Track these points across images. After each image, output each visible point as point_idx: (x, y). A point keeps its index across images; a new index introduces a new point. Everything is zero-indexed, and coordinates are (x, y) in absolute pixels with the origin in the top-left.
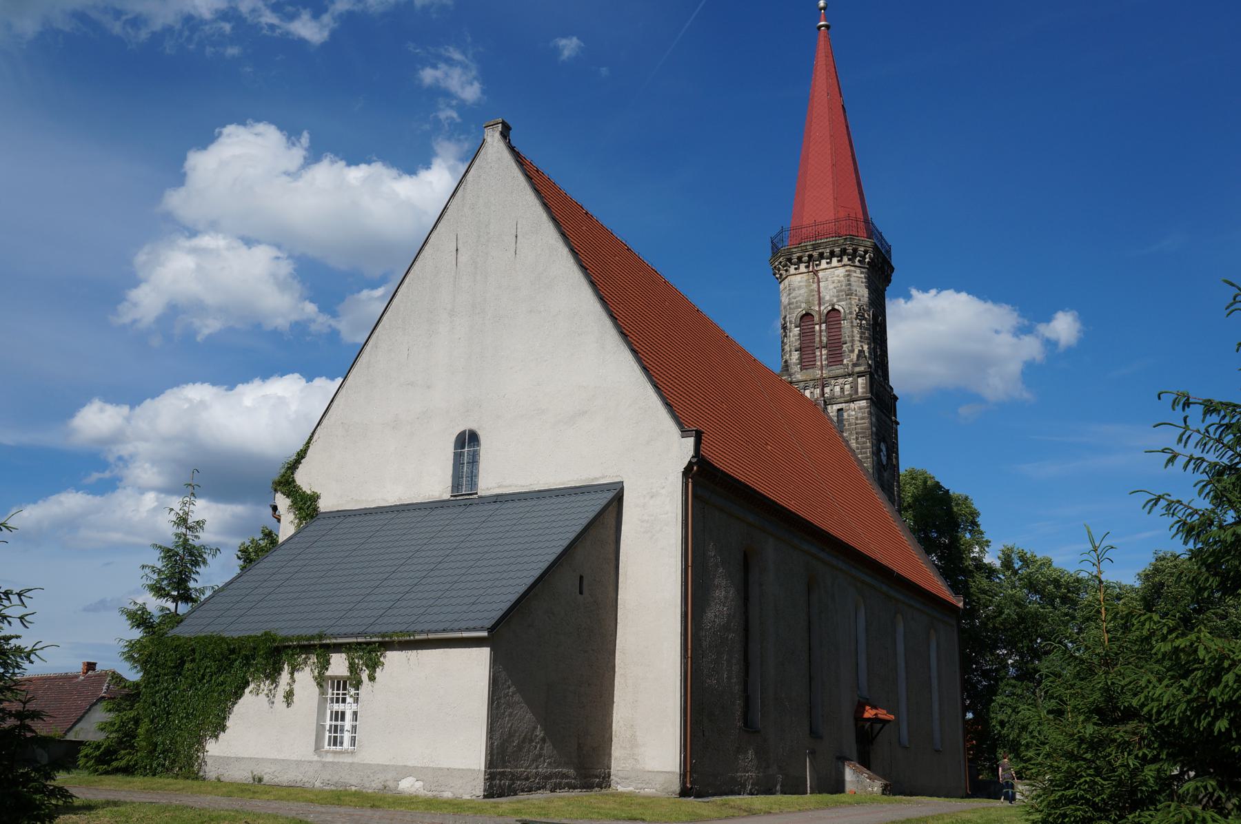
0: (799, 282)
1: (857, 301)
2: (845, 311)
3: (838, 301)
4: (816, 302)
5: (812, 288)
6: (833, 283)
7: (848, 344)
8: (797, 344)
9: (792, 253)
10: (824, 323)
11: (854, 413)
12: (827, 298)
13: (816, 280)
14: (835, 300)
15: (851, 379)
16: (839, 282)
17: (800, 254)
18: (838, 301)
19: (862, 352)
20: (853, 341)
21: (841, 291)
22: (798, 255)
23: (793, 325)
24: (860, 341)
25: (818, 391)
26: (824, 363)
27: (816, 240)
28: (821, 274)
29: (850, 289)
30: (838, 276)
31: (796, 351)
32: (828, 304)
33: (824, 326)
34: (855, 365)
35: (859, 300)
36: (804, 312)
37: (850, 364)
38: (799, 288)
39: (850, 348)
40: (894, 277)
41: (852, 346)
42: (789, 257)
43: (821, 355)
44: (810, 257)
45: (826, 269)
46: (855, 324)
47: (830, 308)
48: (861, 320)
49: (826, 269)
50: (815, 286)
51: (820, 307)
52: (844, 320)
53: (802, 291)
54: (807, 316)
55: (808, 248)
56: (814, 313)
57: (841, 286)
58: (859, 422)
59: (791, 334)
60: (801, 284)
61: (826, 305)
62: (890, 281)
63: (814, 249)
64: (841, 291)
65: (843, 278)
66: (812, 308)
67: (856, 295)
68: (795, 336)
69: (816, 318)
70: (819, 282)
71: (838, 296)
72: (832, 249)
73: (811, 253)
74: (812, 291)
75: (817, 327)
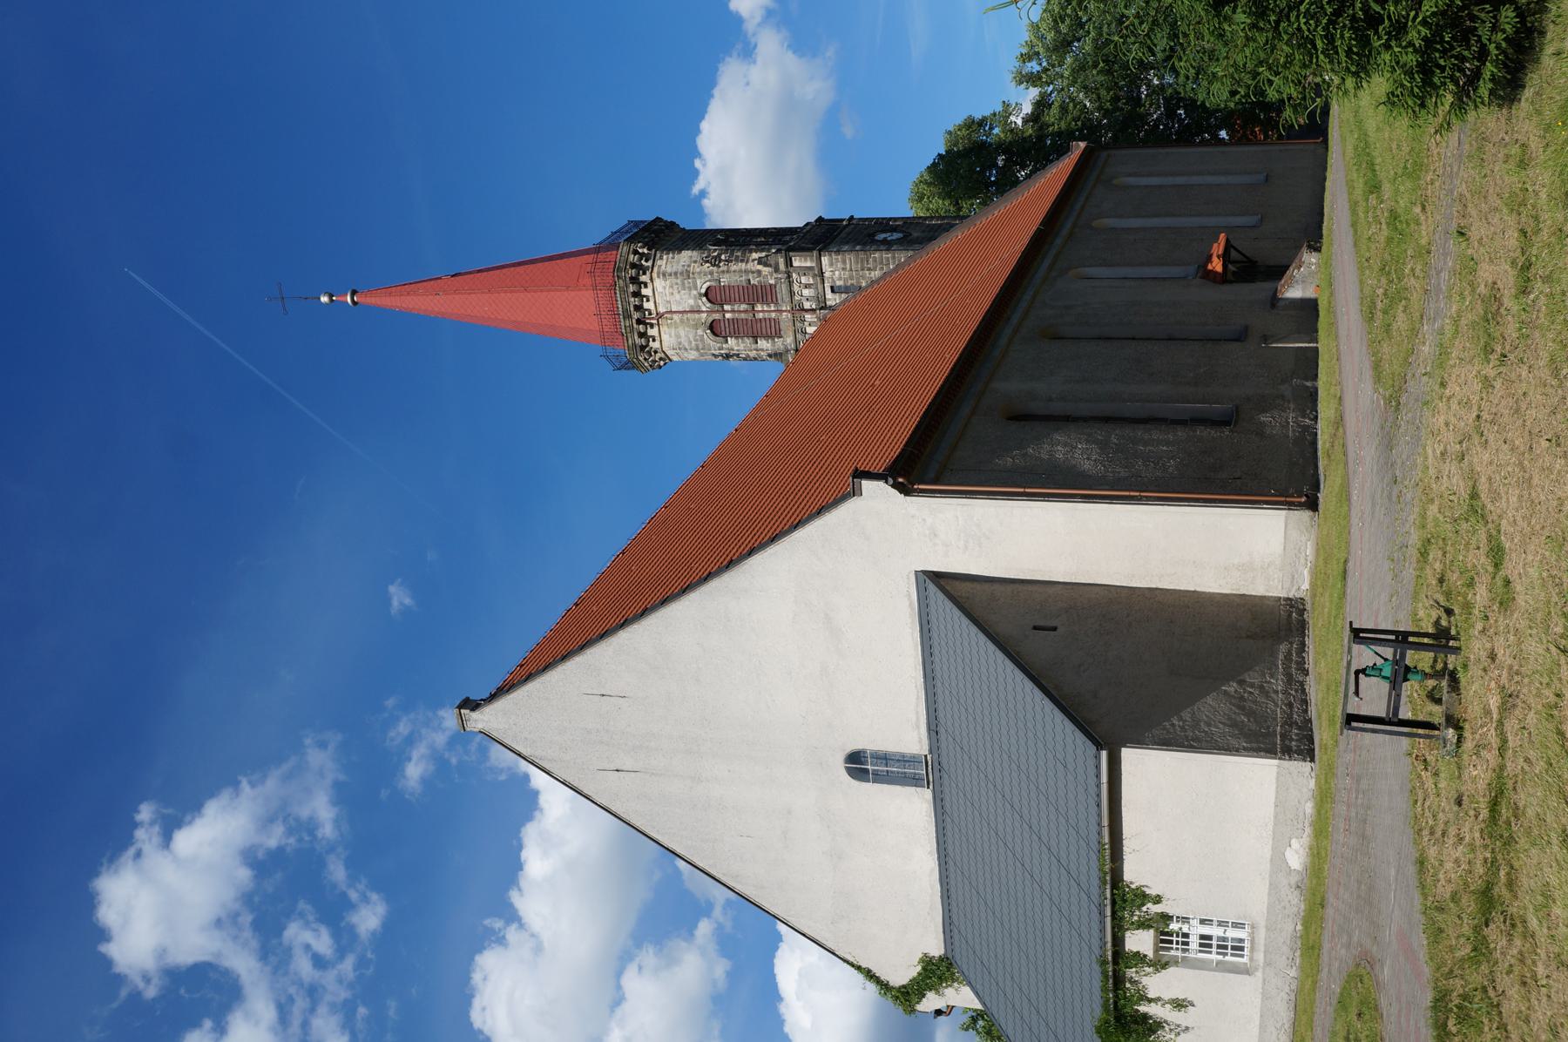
0: (670, 336)
1: (696, 265)
2: (709, 281)
3: (696, 288)
4: (697, 316)
5: (678, 321)
6: (672, 294)
7: (751, 277)
8: (748, 341)
9: (634, 344)
10: (723, 307)
11: (837, 273)
12: (691, 302)
13: (669, 316)
14: (695, 292)
15: (794, 275)
16: (671, 287)
17: (636, 334)
18: (696, 288)
19: (760, 261)
20: (746, 272)
21: (683, 284)
22: (636, 337)
23: (724, 346)
24: (747, 262)
25: (808, 317)
26: (773, 309)
27: (619, 314)
28: (662, 309)
29: (682, 273)
30: (665, 288)
31: (757, 343)
32: (700, 301)
33: (726, 307)
34: (777, 270)
35: (695, 262)
36: (709, 331)
38: (678, 336)
40: (668, 217)
41: (753, 272)
42: (638, 349)
43: (763, 311)
44: (639, 322)
45: (655, 302)
46: (725, 268)
47: (704, 299)
48: (720, 261)
49: (655, 302)
50: (676, 317)
51: (703, 312)
52: (720, 281)
53: (682, 333)
54: (713, 328)
56: (710, 319)
57: (677, 284)
58: (848, 266)
59: (736, 348)
60: (673, 334)
61: (701, 304)
62: (673, 223)
63: (630, 317)
64: (683, 284)
66: (703, 321)
67: (689, 266)
69: (717, 316)
70: (671, 312)
71: (690, 289)
72: (630, 296)
73: (634, 321)
74: (682, 321)
75: (728, 316)
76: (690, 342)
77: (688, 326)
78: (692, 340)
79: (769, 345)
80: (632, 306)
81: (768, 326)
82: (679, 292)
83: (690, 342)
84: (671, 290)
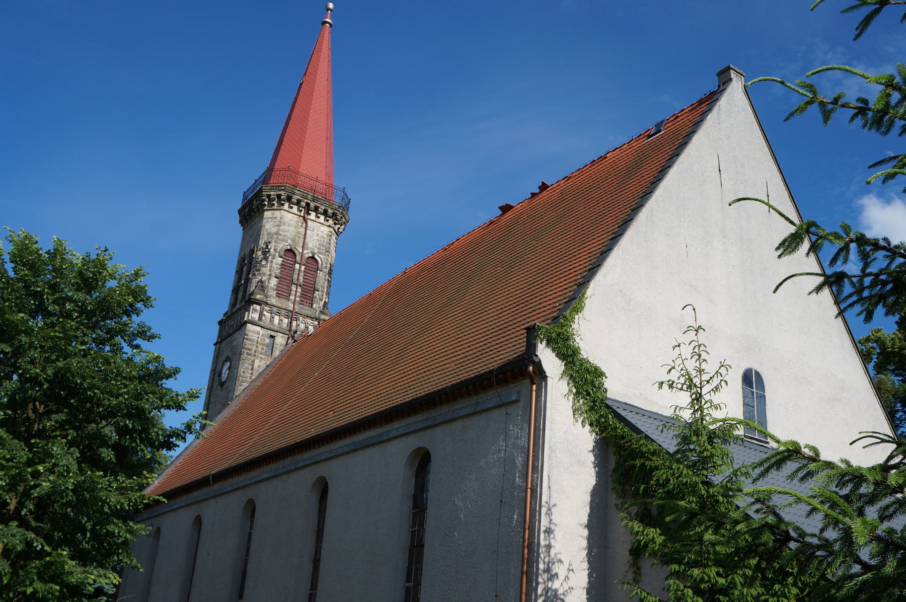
0: (290, 220)
2: (322, 264)
3: (319, 253)
4: (301, 245)
5: (299, 230)
6: (318, 235)
7: (320, 293)
9: (294, 193)
12: (310, 245)
16: (322, 237)
17: (300, 198)
18: (319, 253)
21: (323, 246)
22: (298, 197)
25: (286, 321)
26: (297, 299)
30: (322, 232)
31: (276, 277)
32: (310, 251)
33: (303, 268)
37: (318, 310)
38: (289, 225)
39: (321, 297)
42: (290, 195)
43: (296, 291)
44: (308, 204)
50: (303, 230)
51: (303, 250)
54: (290, 252)
55: (309, 196)
57: (324, 242)
59: (274, 261)
60: (291, 222)
63: (313, 201)
64: (323, 246)
65: (325, 236)
66: (296, 247)
68: (278, 264)
72: (326, 208)
73: (309, 202)
74: (299, 233)
75: (297, 266)
76: (284, 232)
77: (295, 235)
78: (285, 233)
79: (272, 285)
80: (319, 205)
81: (284, 290)
82: (318, 240)
83: (284, 232)
84: (320, 236)
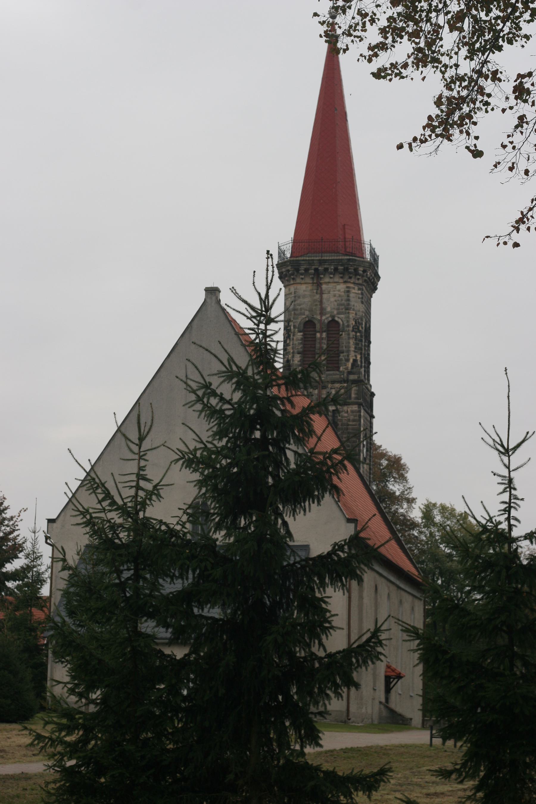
0: (304, 291)
1: (354, 315)
2: (343, 324)
3: (339, 313)
4: (318, 312)
5: (315, 298)
7: (345, 354)
8: (300, 347)
10: (325, 331)
11: (346, 415)
12: (329, 309)
13: (319, 291)
14: (335, 312)
15: (345, 385)
16: (340, 296)
17: (308, 267)
19: (355, 361)
20: (348, 351)
21: (341, 305)
22: (305, 267)
23: (296, 330)
24: (355, 352)
27: (322, 256)
28: (324, 287)
29: (349, 304)
30: (339, 291)
31: (298, 353)
33: (324, 335)
34: (349, 373)
35: (356, 314)
36: (307, 319)
37: (346, 371)
38: (304, 296)
39: (346, 357)
40: (380, 285)
41: (348, 356)
44: (316, 270)
45: (329, 282)
46: (351, 336)
47: (330, 319)
48: (356, 332)
49: (329, 282)
51: (321, 317)
52: (342, 332)
53: (307, 300)
55: (315, 262)
56: (316, 322)
57: (342, 300)
58: (351, 423)
59: (295, 338)
61: (327, 316)
62: (375, 289)
65: (343, 294)
66: (315, 316)
67: (354, 310)
68: (298, 340)
69: (318, 326)
70: (322, 293)
71: (338, 309)
73: (317, 267)
74: (315, 301)
75: (318, 335)
76: (300, 305)
78: (302, 306)
84: (337, 295)
